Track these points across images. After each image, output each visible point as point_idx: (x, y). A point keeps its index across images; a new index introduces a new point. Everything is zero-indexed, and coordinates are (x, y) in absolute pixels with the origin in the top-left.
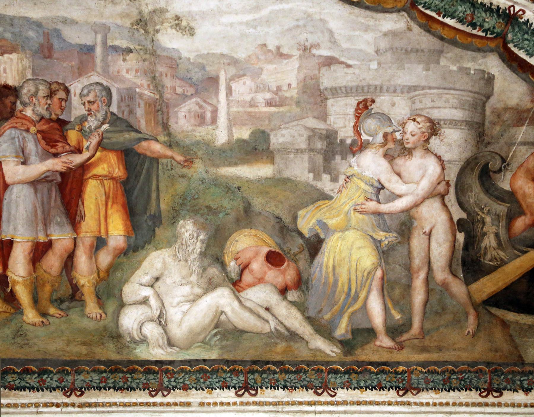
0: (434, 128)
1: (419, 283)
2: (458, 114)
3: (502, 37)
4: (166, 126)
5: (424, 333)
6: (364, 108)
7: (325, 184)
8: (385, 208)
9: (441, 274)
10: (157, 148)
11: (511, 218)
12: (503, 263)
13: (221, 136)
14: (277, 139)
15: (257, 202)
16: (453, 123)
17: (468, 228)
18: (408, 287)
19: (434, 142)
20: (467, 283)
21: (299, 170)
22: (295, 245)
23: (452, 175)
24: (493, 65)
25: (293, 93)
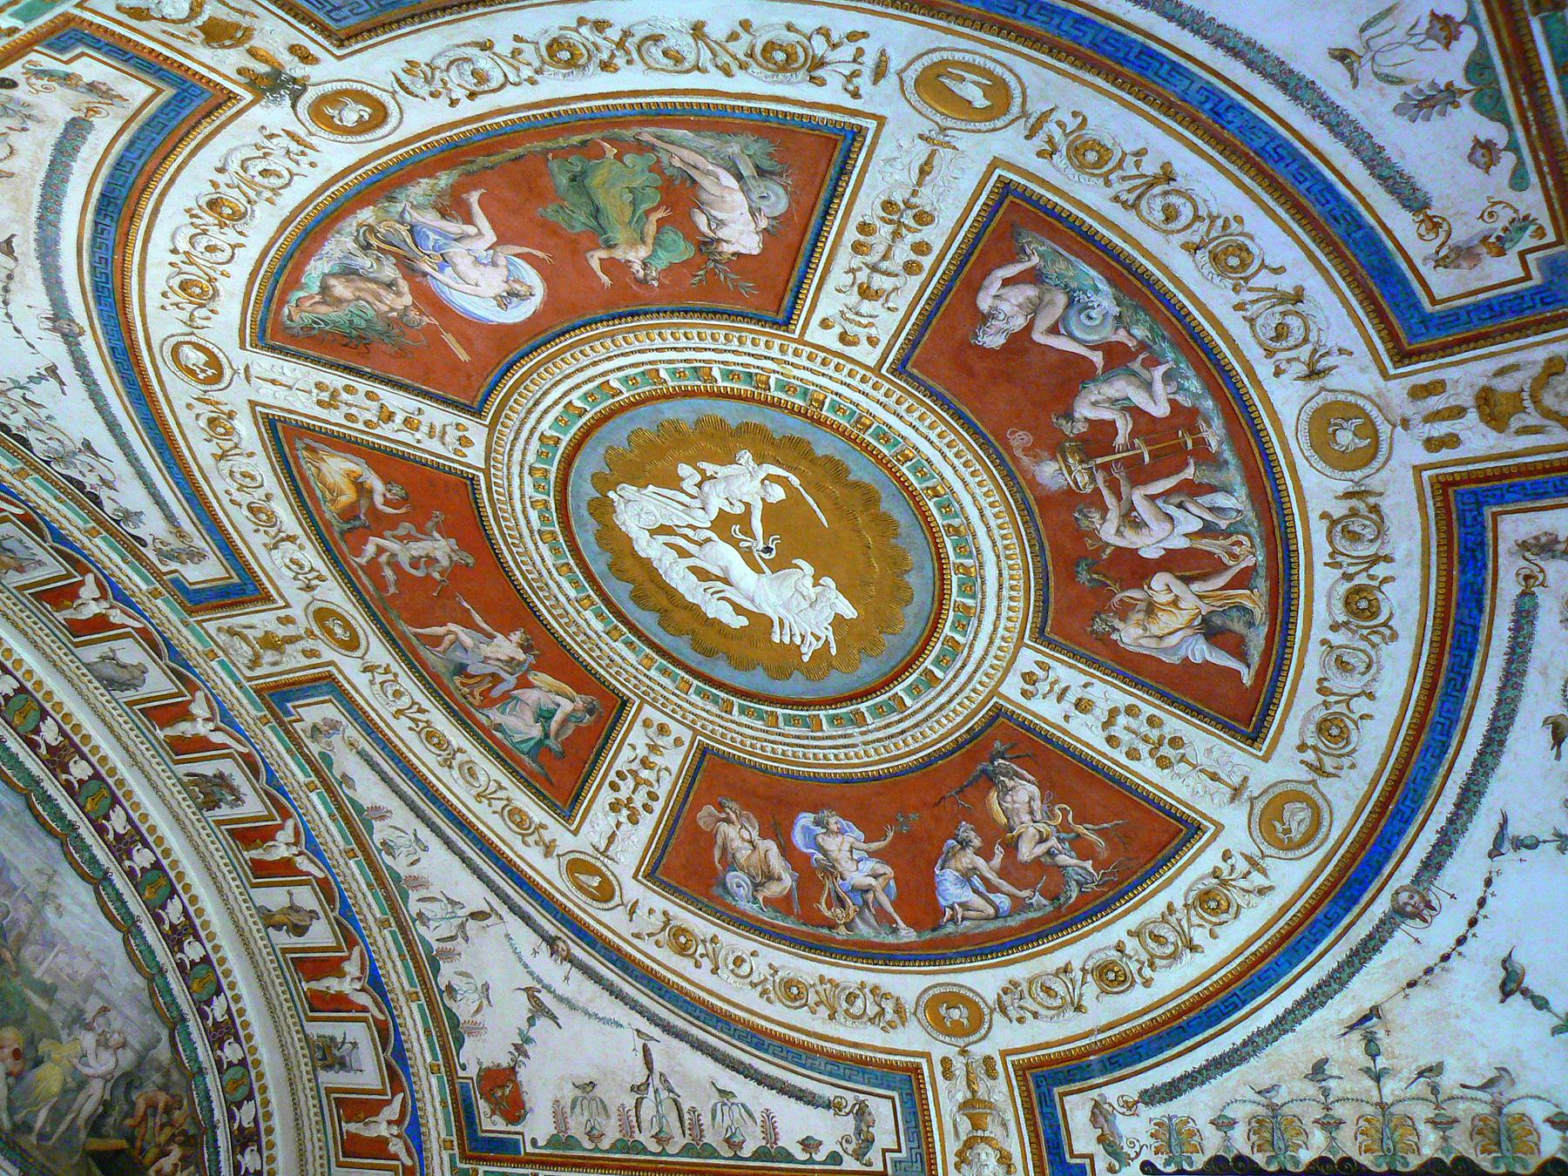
0: (124, 1045)
1: (69, 1117)
2: (138, 1046)
3: (175, 1024)
4: (19, 950)
5: (54, 1147)
6: (104, 1010)
7: (64, 1034)
8: (80, 1067)
9: (80, 1122)
10: (8, 956)
11: (128, 1115)
12: (109, 1137)
13: (38, 974)
14: (58, 995)
15: (30, 1019)
16: (133, 1049)
17: (107, 1105)
18: (62, 1117)
19: (120, 1051)
20: (88, 1135)
21: (58, 1018)
22: (30, 1055)
23: (117, 1075)
24: (165, 1034)
25: (80, 979)
